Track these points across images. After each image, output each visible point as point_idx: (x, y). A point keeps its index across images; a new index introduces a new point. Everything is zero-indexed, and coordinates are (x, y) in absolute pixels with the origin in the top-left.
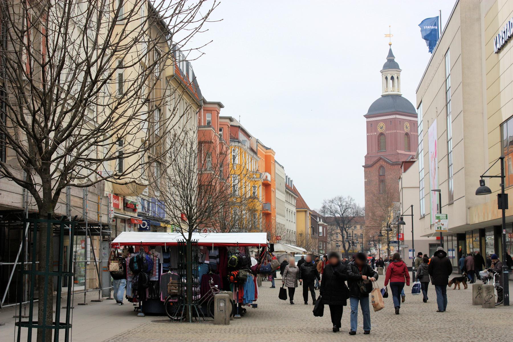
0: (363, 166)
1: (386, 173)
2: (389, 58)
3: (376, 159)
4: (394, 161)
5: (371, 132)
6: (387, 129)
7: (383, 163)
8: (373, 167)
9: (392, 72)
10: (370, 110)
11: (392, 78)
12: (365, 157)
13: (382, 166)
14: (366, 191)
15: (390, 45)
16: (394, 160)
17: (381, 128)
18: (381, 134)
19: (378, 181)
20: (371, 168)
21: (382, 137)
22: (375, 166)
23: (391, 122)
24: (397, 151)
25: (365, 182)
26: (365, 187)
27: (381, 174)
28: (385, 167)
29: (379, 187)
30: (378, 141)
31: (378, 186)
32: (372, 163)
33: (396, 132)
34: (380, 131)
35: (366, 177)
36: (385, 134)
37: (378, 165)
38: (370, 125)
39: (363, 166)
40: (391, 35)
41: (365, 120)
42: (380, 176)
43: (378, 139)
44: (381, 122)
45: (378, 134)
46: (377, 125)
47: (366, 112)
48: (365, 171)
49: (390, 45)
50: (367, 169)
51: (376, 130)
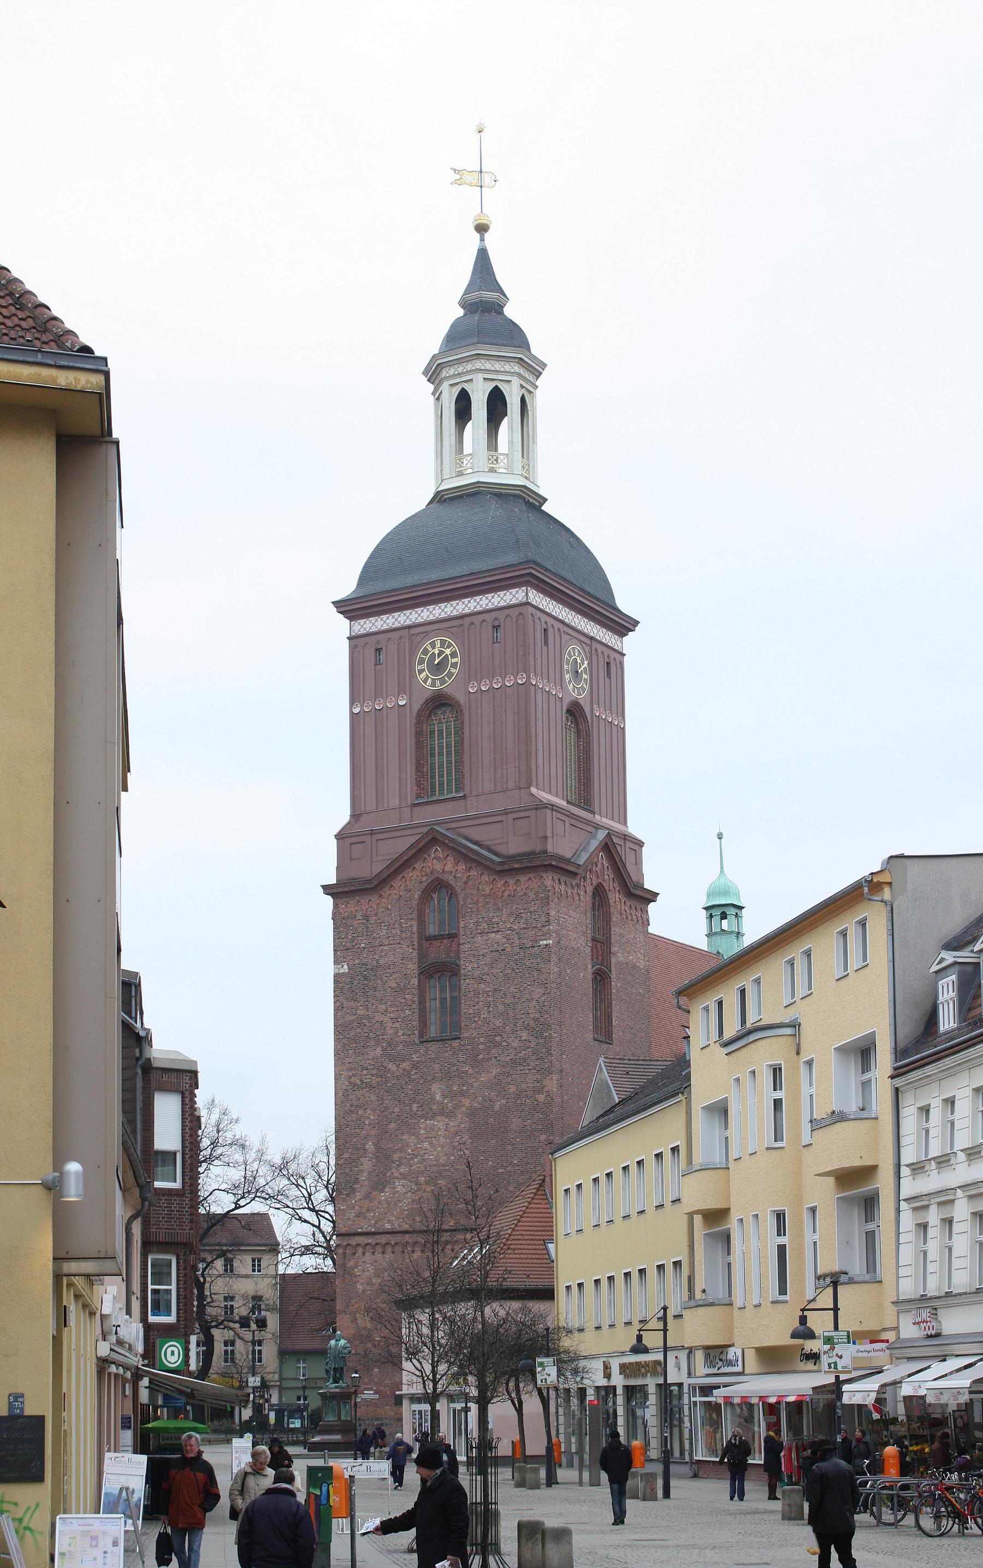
0: (327, 889)
1: (467, 923)
2: (474, 295)
3: (402, 845)
4: (513, 850)
5: (378, 693)
6: (471, 671)
7: (449, 866)
8: (386, 891)
9: (498, 366)
10: (369, 572)
11: (497, 405)
12: (340, 837)
13: (438, 885)
14: (341, 1030)
15: (482, 229)
16: (515, 846)
17: (437, 668)
18: (439, 702)
19: (413, 967)
20: (374, 898)
21: (443, 721)
22: (397, 883)
23: (496, 628)
24: (534, 790)
25: (338, 978)
26: (339, 1009)
27: (432, 930)
28: (458, 886)
29: (422, 1002)
30: (419, 745)
31: (412, 996)
32: (377, 868)
33: (528, 683)
34: (426, 681)
35: (342, 950)
36: (460, 697)
37: (415, 878)
38: (370, 653)
39: (327, 889)
40: (487, 179)
41: (342, 626)
42: (429, 939)
43: (418, 734)
44: (439, 632)
45: (417, 706)
46: (413, 654)
47: (347, 586)
48: (337, 916)
49: (482, 229)
50: (351, 906)
51: (405, 683)
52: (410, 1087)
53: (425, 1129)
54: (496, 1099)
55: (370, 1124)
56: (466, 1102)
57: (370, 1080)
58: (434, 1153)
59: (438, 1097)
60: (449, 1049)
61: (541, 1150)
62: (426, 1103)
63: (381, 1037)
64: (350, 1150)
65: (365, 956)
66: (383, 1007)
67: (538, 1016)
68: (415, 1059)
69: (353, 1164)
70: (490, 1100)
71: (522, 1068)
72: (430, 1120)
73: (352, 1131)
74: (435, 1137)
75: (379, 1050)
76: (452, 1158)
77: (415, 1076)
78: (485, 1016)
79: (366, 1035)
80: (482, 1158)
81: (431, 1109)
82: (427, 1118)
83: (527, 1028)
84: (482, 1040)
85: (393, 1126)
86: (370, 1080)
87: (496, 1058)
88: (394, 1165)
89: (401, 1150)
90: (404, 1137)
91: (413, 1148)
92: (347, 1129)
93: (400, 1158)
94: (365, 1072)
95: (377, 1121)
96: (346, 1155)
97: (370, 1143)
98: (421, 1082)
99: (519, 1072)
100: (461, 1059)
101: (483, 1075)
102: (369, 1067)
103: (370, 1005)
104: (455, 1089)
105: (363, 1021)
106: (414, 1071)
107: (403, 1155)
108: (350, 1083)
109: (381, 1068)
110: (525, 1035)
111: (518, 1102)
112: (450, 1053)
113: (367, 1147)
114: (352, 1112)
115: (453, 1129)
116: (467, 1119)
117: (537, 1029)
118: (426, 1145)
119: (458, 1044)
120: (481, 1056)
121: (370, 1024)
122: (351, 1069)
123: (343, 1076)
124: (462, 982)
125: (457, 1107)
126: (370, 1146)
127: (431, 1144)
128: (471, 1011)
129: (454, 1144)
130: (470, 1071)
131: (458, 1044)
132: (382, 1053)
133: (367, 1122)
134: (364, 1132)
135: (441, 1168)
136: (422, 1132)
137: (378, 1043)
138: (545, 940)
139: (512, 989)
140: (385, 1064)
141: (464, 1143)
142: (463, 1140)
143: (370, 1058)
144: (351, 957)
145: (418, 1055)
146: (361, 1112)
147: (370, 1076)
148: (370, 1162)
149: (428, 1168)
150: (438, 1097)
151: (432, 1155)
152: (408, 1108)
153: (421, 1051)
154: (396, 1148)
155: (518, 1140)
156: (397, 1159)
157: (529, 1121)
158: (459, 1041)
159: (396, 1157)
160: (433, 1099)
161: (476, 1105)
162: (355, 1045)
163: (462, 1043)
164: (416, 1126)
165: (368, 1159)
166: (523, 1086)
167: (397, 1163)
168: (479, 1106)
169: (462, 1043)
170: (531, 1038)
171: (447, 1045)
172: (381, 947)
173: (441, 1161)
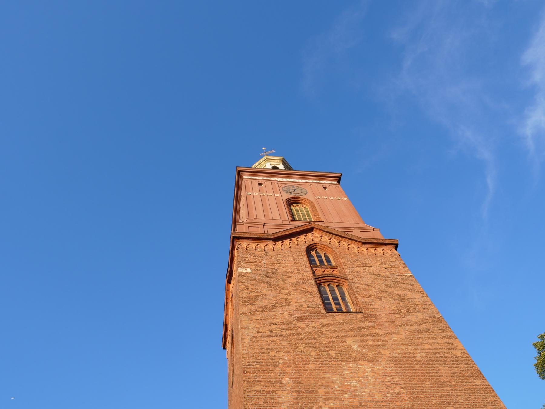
52: (323, 339)
53: (349, 370)
54: (415, 352)
55: (284, 363)
56: (387, 353)
57: (280, 332)
58: (366, 390)
59: (355, 347)
60: (354, 318)
61: (482, 392)
62: (343, 351)
63: (287, 307)
64: (262, 384)
65: (265, 266)
66: (287, 291)
67: (424, 306)
68: (323, 321)
69: (268, 396)
70: (410, 353)
71: (429, 334)
72: (352, 363)
73: (264, 368)
74: (362, 377)
75: (286, 315)
76: (388, 395)
77: (328, 333)
78: (380, 303)
79: (273, 304)
80: (422, 396)
81: (351, 356)
82: (348, 362)
83: (419, 311)
84: (383, 315)
85: (311, 366)
86: (280, 332)
87: (401, 326)
88: (320, 399)
89: (326, 386)
90: (327, 376)
91: (340, 385)
92: (258, 366)
93: (327, 394)
94: (274, 326)
95: (292, 361)
96: (258, 388)
97: (287, 379)
98: (335, 336)
99: (427, 336)
100: (369, 325)
101: (394, 335)
102: (277, 323)
103: (273, 289)
104: (371, 343)
105: (268, 297)
106: (325, 329)
107: (329, 390)
108: (259, 332)
109: (290, 325)
110: (420, 316)
111: (438, 355)
112: (357, 320)
113: (284, 381)
114: (263, 353)
115: (380, 372)
116: (392, 365)
117: (429, 313)
118: (354, 383)
119: (362, 316)
120: (387, 325)
121: (275, 299)
122: (258, 324)
123: (250, 327)
124: (352, 285)
125: (378, 355)
126: (286, 380)
127: (360, 382)
128: (366, 300)
129: (386, 383)
130: (381, 333)
131: (362, 316)
132: (290, 316)
133: (281, 361)
134: (277, 369)
135: (378, 404)
136: (346, 372)
137: (284, 309)
138: (408, 273)
139: (395, 292)
140: (295, 323)
141: (397, 383)
142: (395, 380)
143: (278, 318)
144: (254, 266)
145: (326, 319)
146: (273, 353)
147: (279, 329)
148: (289, 396)
149: (363, 404)
150: (355, 347)
151: (365, 392)
152: (325, 353)
153: (329, 318)
154: (319, 384)
155: (454, 383)
156: (323, 394)
157: (456, 369)
158: (362, 314)
159: (321, 392)
160: (350, 347)
161: (397, 355)
162: (262, 309)
163: (365, 315)
164: (338, 368)
165: (286, 392)
166: (436, 345)
167: (324, 397)
168: (400, 356)
169: (365, 315)
170: (426, 317)
171: (351, 316)
172: (279, 264)
173: (376, 397)
